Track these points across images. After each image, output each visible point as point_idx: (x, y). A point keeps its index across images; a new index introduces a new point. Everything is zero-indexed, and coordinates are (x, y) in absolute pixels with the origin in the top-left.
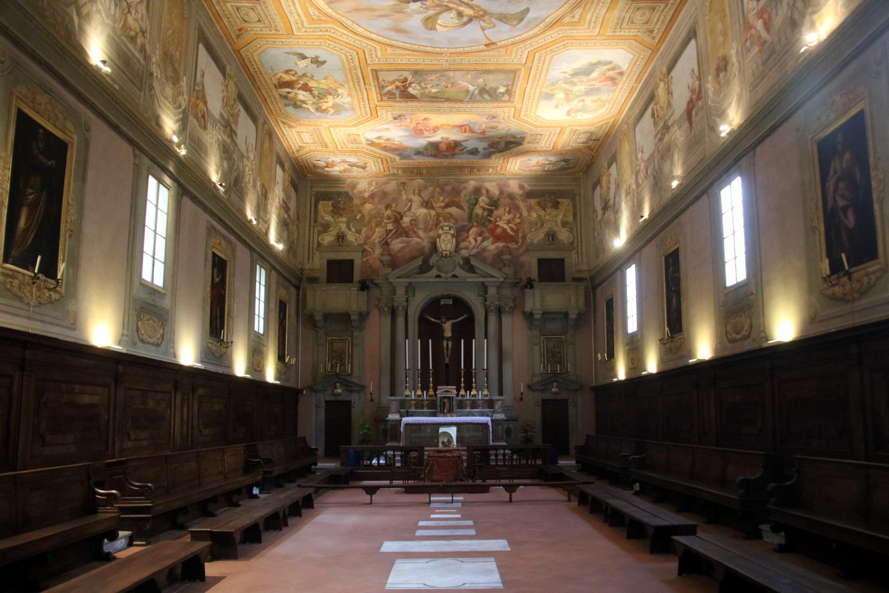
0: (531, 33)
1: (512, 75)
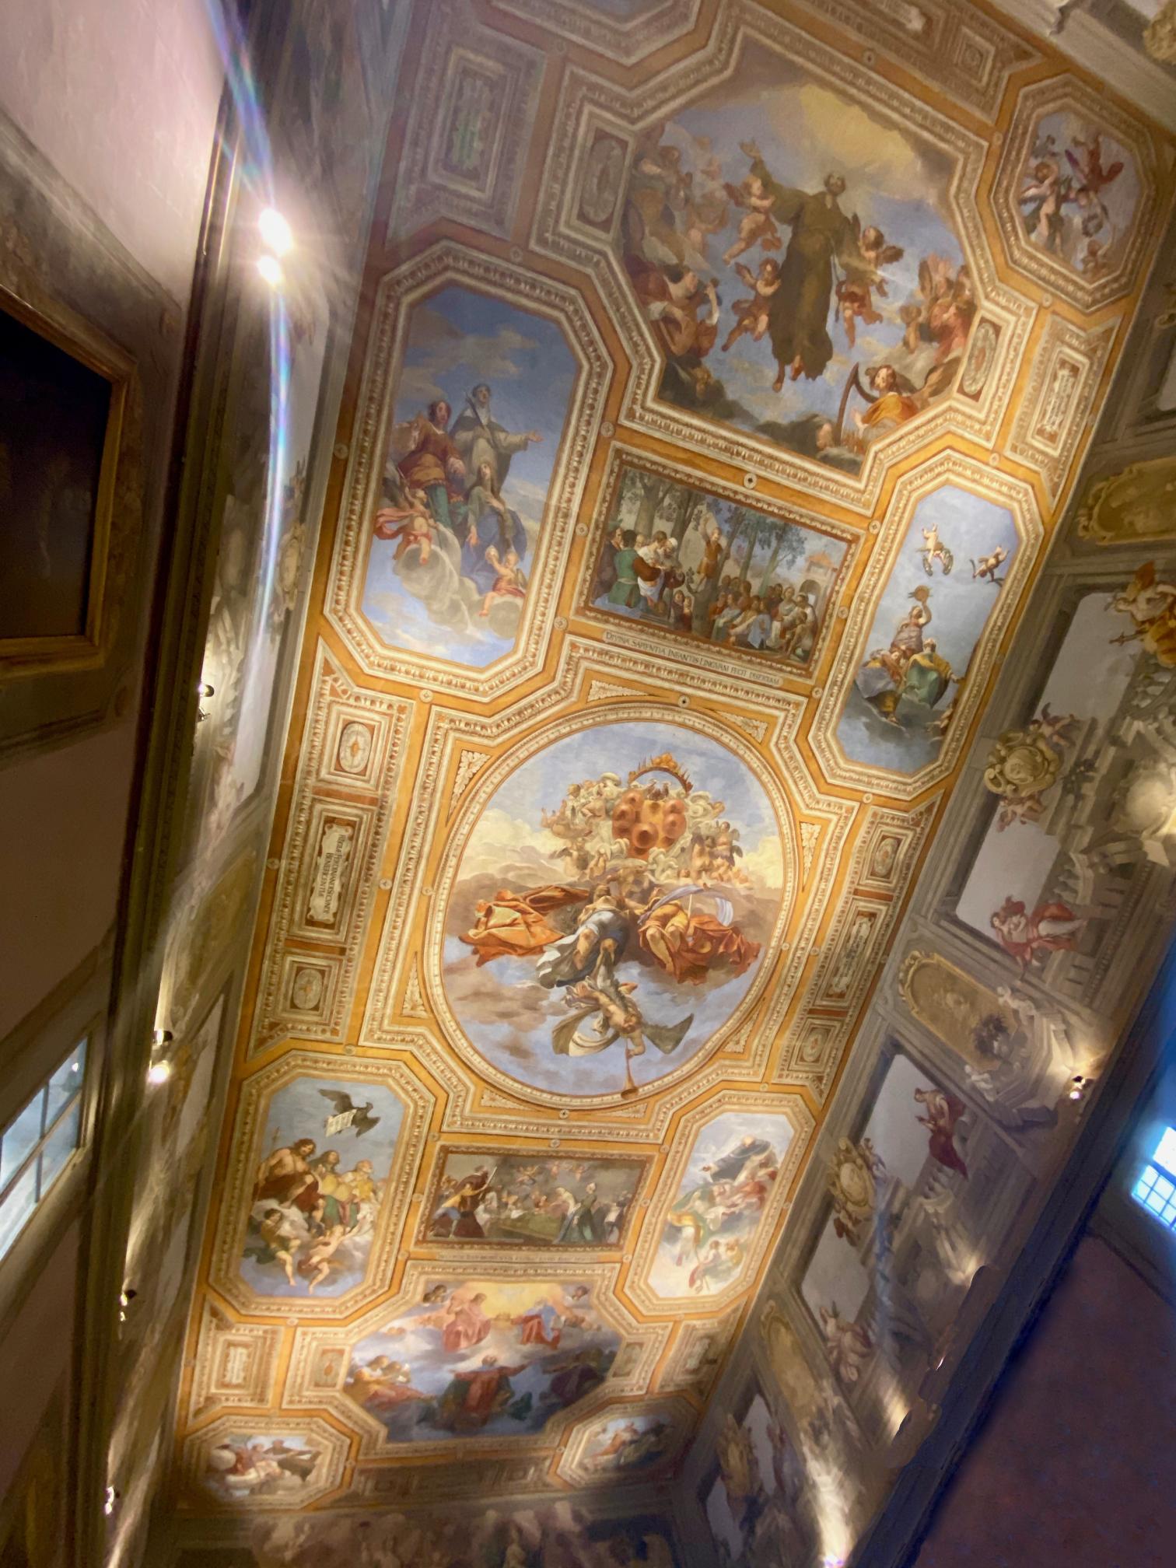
0: (687, 1068)
1: (637, 1172)
